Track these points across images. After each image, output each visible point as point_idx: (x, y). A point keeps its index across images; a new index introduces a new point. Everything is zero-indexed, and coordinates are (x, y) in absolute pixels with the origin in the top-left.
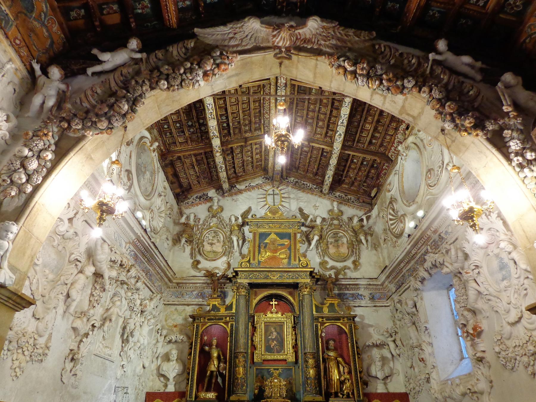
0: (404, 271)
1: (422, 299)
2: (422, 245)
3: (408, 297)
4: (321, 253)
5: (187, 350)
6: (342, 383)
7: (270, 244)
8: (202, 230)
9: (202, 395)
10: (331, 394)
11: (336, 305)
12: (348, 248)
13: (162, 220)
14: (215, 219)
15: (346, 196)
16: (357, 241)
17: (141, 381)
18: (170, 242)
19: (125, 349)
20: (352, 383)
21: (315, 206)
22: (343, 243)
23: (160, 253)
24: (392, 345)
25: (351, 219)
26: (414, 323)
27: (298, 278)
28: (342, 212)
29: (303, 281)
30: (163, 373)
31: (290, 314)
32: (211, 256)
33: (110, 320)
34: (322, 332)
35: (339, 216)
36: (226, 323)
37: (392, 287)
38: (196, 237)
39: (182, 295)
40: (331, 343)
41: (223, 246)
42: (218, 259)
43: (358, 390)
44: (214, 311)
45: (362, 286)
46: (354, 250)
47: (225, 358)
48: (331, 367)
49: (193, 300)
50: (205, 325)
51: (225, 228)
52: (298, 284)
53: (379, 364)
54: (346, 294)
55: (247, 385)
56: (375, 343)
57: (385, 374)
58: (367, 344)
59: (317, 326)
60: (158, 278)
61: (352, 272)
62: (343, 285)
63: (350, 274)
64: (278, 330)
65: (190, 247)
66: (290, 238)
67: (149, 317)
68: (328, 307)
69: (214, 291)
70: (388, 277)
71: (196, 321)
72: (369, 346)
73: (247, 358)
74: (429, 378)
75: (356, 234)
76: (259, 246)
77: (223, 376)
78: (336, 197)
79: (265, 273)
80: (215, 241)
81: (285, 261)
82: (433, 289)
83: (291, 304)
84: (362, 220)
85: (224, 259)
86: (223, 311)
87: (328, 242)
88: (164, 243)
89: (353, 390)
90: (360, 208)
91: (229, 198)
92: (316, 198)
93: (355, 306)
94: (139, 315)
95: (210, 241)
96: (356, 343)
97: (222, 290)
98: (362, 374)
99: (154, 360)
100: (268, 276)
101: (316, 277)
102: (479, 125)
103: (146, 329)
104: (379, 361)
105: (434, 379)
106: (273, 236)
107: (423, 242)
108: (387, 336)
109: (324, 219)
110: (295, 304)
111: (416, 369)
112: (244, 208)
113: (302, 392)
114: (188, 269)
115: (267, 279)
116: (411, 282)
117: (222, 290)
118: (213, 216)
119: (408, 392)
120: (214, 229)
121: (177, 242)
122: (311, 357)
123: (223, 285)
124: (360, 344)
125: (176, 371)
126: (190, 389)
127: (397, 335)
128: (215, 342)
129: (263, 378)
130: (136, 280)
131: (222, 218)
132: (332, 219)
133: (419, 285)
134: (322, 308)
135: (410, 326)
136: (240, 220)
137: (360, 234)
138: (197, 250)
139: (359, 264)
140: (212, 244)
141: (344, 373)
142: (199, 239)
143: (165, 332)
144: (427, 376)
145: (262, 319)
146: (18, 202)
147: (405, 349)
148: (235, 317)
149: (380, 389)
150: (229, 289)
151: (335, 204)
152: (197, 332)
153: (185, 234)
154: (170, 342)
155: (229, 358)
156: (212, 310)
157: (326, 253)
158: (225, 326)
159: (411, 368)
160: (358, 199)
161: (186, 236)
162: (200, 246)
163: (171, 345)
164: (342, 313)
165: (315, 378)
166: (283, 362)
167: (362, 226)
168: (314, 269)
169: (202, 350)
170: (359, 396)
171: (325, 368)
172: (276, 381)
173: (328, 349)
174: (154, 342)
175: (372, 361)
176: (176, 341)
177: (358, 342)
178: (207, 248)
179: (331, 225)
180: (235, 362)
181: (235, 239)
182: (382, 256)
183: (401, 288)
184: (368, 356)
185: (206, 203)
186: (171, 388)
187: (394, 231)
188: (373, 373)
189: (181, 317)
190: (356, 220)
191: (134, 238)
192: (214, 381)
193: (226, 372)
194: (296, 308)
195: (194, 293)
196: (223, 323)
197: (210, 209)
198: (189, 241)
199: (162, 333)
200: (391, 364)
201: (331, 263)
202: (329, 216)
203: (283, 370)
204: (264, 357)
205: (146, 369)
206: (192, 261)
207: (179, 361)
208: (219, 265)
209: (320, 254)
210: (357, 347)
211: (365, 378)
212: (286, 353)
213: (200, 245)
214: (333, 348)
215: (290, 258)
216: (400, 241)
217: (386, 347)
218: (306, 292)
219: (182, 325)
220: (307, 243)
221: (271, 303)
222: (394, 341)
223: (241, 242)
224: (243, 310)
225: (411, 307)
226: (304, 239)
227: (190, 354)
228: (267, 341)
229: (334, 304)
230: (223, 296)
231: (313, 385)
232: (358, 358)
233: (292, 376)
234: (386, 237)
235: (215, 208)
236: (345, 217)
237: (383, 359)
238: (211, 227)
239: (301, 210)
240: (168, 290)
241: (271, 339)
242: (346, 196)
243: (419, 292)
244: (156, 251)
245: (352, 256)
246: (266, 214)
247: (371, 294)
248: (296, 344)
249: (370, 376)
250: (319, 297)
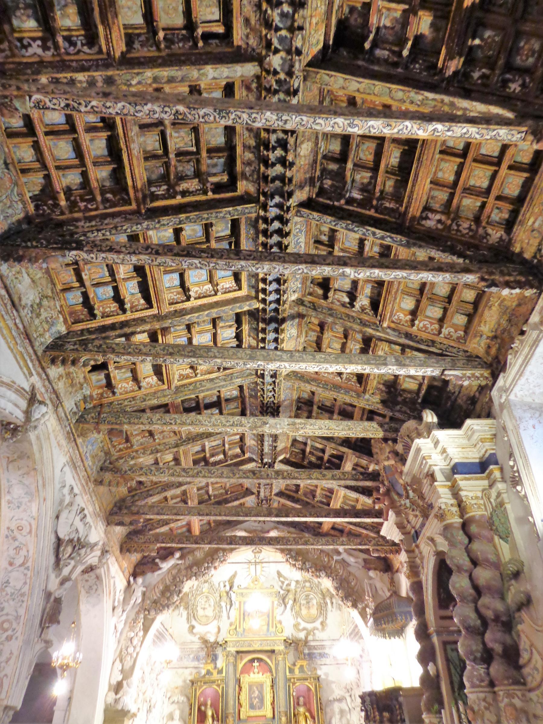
14: (206, 585)
24: (349, 699)
36: (218, 686)
40: (301, 699)
47: (218, 717)
53: (338, 717)
63: (319, 635)
80: (207, 606)
85: (215, 622)
86: (215, 676)
102: (355, 606)
109: (297, 582)
110: (273, 667)
128: (209, 703)
136: (228, 588)
140: (204, 609)
145: (246, 680)
146: (131, 664)
150: (219, 652)
169: (199, 709)
173: (298, 704)
178: (201, 612)
179: (303, 587)
181: (223, 604)
198: (186, 608)
200: (348, 717)
201: (303, 625)
215: (268, 625)
223: (228, 607)
227: (190, 714)
228: (251, 699)
230: (215, 659)
237: (342, 712)
239: (279, 574)
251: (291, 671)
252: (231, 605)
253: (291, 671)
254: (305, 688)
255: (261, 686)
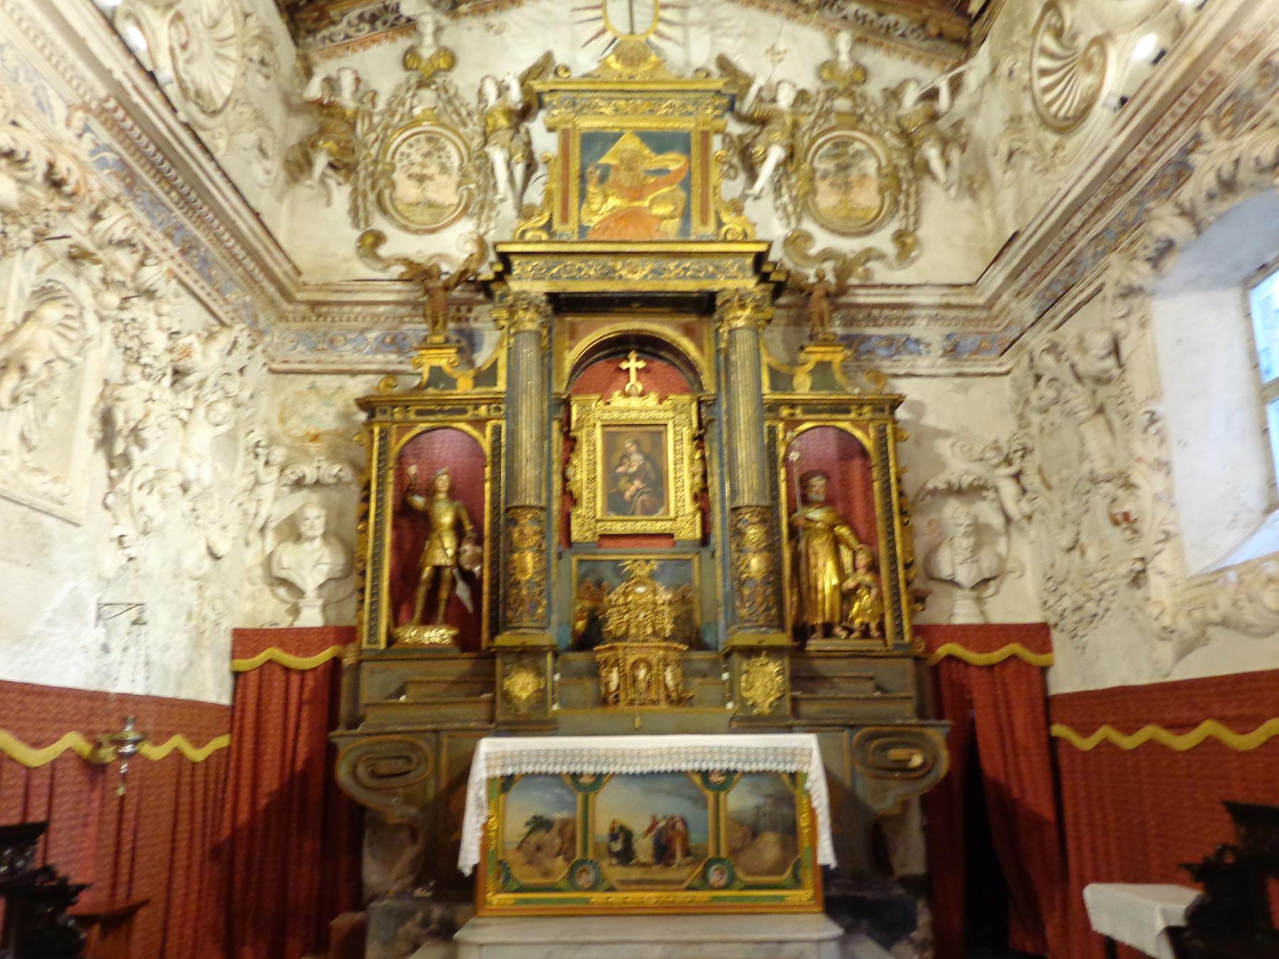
0: (1081, 243)
1: (1144, 324)
2: (1175, 126)
3: (1089, 329)
4: (790, 209)
5: (353, 509)
6: (847, 596)
7: (617, 169)
8: (386, 129)
9: (410, 634)
10: (813, 629)
11: (836, 366)
12: (881, 191)
13: (232, 70)
14: (428, 95)
15: (881, 15)
16: (912, 164)
17: (208, 594)
18: (275, 165)
19: (124, 485)
20: (880, 597)
21: (772, 51)
22: (865, 176)
23: (225, 175)
24: (1008, 490)
25: (894, 95)
26: (1101, 410)
27: (713, 276)
28: (863, 73)
29: (732, 284)
30: (283, 574)
31: (686, 398)
32: (422, 216)
33: (23, 369)
34: (789, 449)
35: (857, 83)
36: (479, 423)
37: (1026, 310)
38: (364, 153)
39: (332, 341)
40: (818, 483)
41: (459, 185)
42: (443, 227)
43: (898, 617)
44: (436, 386)
45: (924, 312)
46: (902, 198)
48: (816, 554)
49: (369, 357)
50: (409, 429)
51: (465, 125)
52: (712, 295)
53: (965, 543)
54: (870, 337)
55: (549, 606)
56: (954, 480)
57: (980, 571)
58: (930, 486)
59: (772, 430)
60: (237, 278)
61: (891, 268)
62: (860, 307)
64: (647, 449)
65: (347, 189)
66: (687, 151)
67: (213, 398)
68: (811, 372)
69: (435, 323)
70: (1015, 275)
71: (379, 417)
72: (934, 492)
73: (549, 523)
74: (1143, 571)
75: (910, 144)
76: (583, 178)
77: (472, 581)
78: (845, 17)
79: (602, 260)
80: (433, 169)
81: (672, 227)
82: (1194, 284)
83: (691, 366)
84: (932, 95)
85: (466, 227)
87: (814, 171)
88: (249, 163)
89: (882, 616)
90: (925, 58)
91: (476, 23)
92: (778, 21)
93: (896, 376)
94: (167, 381)
95: (416, 170)
96: (899, 481)
97: (463, 325)
98: (912, 574)
99: (253, 536)
100: (615, 271)
101: (773, 277)
103: (203, 434)
104: (967, 535)
105: (1162, 573)
106: (629, 143)
107: (1181, 111)
108: (995, 461)
109: (802, 96)
111: (1092, 554)
112: (528, 57)
113: (722, 622)
114: (347, 260)
115: (612, 279)
116: (1109, 272)
117: (463, 325)
118: (422, 84)
119: (1052, 621)
120: (426, 126)
121: (302, 171)
122: (755, 519)
123: (464, 308)
124: (910, 487)
125: (325, 568)
126: (371, 619)
127: (1027, 458)
128: (443, 482)
129: (599, 584)
130: (137, 257)
131: (452, 91)
132: (831, 94)
133: (1141, 273)
134: (792, 377)
135: (1089, 419)
137: (922, 141)
138: (373, 198)
139: (917, 242)
140: (421, 179)
141: (855, 569)
142: (375, 162)
143: (279, 455)
144: (1138, 566)
147: (1055, 496)
148: (507, 404)
149: (963, 612)
151: (844, 40)
152: (383, 453)
153: (330, 141)
154: (299, 484)
155: (492, 528)
156: (428, 385)
157: (805, 207)
158: (475, 433)
159: (1071, 549)
160: (923, 25)
161: (330, 144)
162: (382, 182)
163: (305, 492)
164: (857, 391)
165: (766, 581)
166: (664, 542)
167: (934, 117)
168: (770, 244)
170: (900, 634)
171: (796, 557)
172: (640, 590)
174: (247, 481)
175: (941, 537)
176: (318, 483)
177: (907, 477)
178: (407, 190)
179: (826, 113)
180: (509, 536)
181: (498, 156)
182: (994, 214)
183: (1059, 305)
184: (930, 523)
185: (393, 40)
186: (312, 617)
187: (1054, 108)
188: (945, 569)
189: (332, 411)
190: (911, 97)
191: (102, 91)
192: (444, 594)
193: (482, 569)
194: (707, 379)
195: (372, 336)
196: (470, 422)
197: (409, 59)
198: (343, 166)
199: (272, 458)
200: (1002, 546)
201: (823, 241)
202: (818, 84)
203: (664, 564)
204: (601, 528)
205: (224, 563)
206: (357, 234)
207: (333, 540)
208: (453, 246)
209: (785, 209)
210: (901, 494)
211: (918, 584)
212: (672, 515)
213: (381, 179)
214: (821, 498)
215: (686, 216)
216: (1073, 142)
217: (990, 494)
218: (741, 318)
219: (337, 434)
220: (742, 177)
221: (624, 366)
222: (1017, 476)
223: (519, 170)
224: (530, 380)
225: (1104, 352)
226: (735, 160)
227: (365, 517)
228: (612, 478)
229: (829, 363)
230: (467, 344)
231: (759, 599)
232: (904, 525)
233: (690, 580)
234: (1016, 145)
235: (427, 52)
236: (874, 89)
237: (979, 531)
238: (415, 122)
240: (283, 325)
241: (626, 474)
242: (881, 15)
243: (1136, 302)
244: (210, 167)
245: (892, 214)
246: (604, 65)
247: (949, 337)
248: (705, 490)
249: (931, 578)
250: (781, 348)
251: (781, 380)
252: (531, 167)
253: (781, 380)
254: (828, 448)
255: (653, 434)
